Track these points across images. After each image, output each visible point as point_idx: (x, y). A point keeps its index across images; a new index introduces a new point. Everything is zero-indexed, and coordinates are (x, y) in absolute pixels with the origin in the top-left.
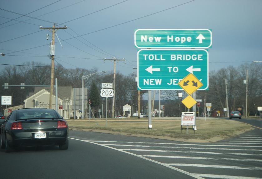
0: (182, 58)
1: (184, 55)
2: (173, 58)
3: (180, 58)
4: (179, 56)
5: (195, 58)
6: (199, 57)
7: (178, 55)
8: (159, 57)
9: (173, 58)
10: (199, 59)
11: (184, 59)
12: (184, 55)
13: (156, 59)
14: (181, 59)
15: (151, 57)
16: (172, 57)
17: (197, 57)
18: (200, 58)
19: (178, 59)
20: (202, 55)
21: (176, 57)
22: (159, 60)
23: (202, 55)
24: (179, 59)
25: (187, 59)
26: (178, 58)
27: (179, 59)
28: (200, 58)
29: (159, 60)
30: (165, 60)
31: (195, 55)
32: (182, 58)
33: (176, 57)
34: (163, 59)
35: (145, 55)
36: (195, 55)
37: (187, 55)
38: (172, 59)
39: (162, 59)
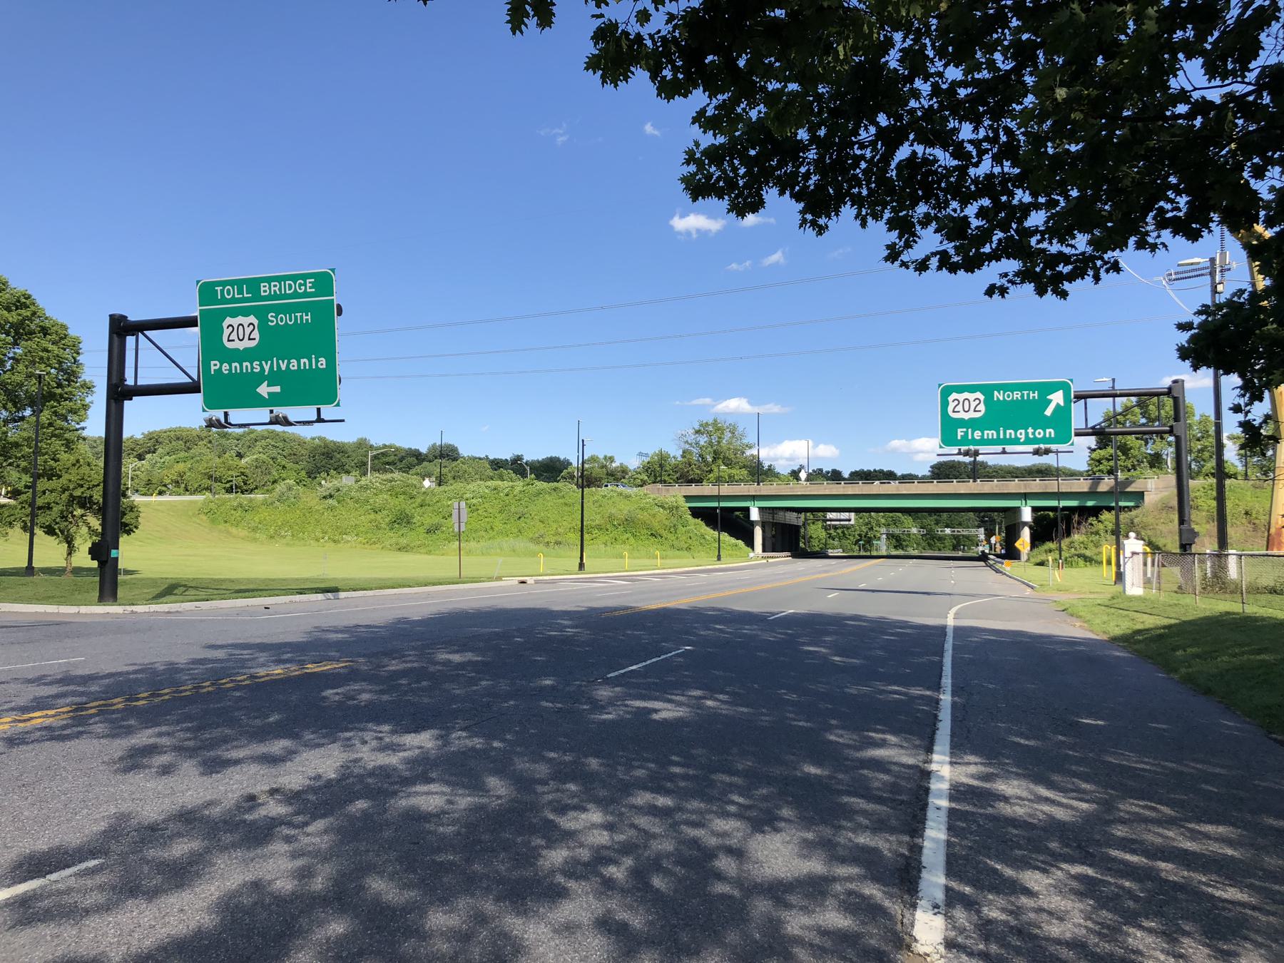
0: (280, 289)
3: (277, 289)
4: (275, 286)
6: (308, 285)
7: (272, 284)
8: (240, 292)
9: (265, 291)
10: (308, 290)
13: (236, 296)
16: (262, 289)
17: (305, 285)
18: (310, 288)
20: (313, 280)
21: (270, 288)
23: (313, 280)
24: (275, 291)
25: (288, 292)
26: (273, 289)
27: (275, 291)
28: (310, 288)
32: (280, 289)
33: (270, 288)
35: (219, 289)
37: (287, 282)
38: (262, 294)
39: (245, 295)
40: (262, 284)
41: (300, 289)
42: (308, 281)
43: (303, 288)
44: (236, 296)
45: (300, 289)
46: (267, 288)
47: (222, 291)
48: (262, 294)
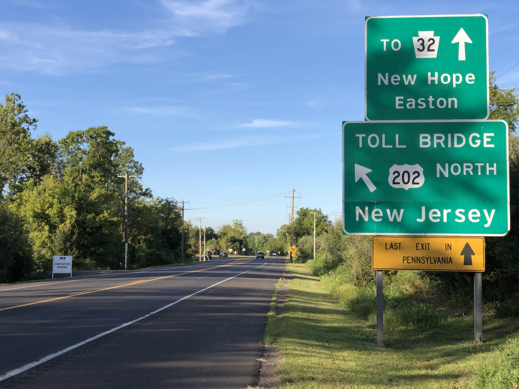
1: (449, 135)
2: (426, 143)
3: (441, 141)
5: (476, 141)
6: (486, 140)
7: (435, 136)
8: (390, 141)
9: (425, 143)
10: (485, 145)
11: (450, 146)
12: (449, 135)
13: (384, 146)
14: (443, 146)
15: (374, 141)
16: (421, 140)
17: (481, 139)
18: (488, 143)
19: (435, 146)
20: (493, 135)
21: (432, 140)
22: (391, 146)
23: (493, 135)
24: (439, 144)
26: (436, 141)
27: (439, 144)
28: (488, 143)
29: (391, 146)
30: (405, 147)
31: (478, 136)
32: (446, 142)
33: (432, 140)
34: (399, 145)
35: (361, 136)
36: (478, 136)
37: (456, 135)
38: (421, 146)
39: (397, 146)
40: (421, 136)
41: (475, 143)
42: (485, 135)
43: (479, 142)
44: (384, 146)
45: (475, 143)
46: (428, 140)
47: (365, 140)
48: (421, 146)
